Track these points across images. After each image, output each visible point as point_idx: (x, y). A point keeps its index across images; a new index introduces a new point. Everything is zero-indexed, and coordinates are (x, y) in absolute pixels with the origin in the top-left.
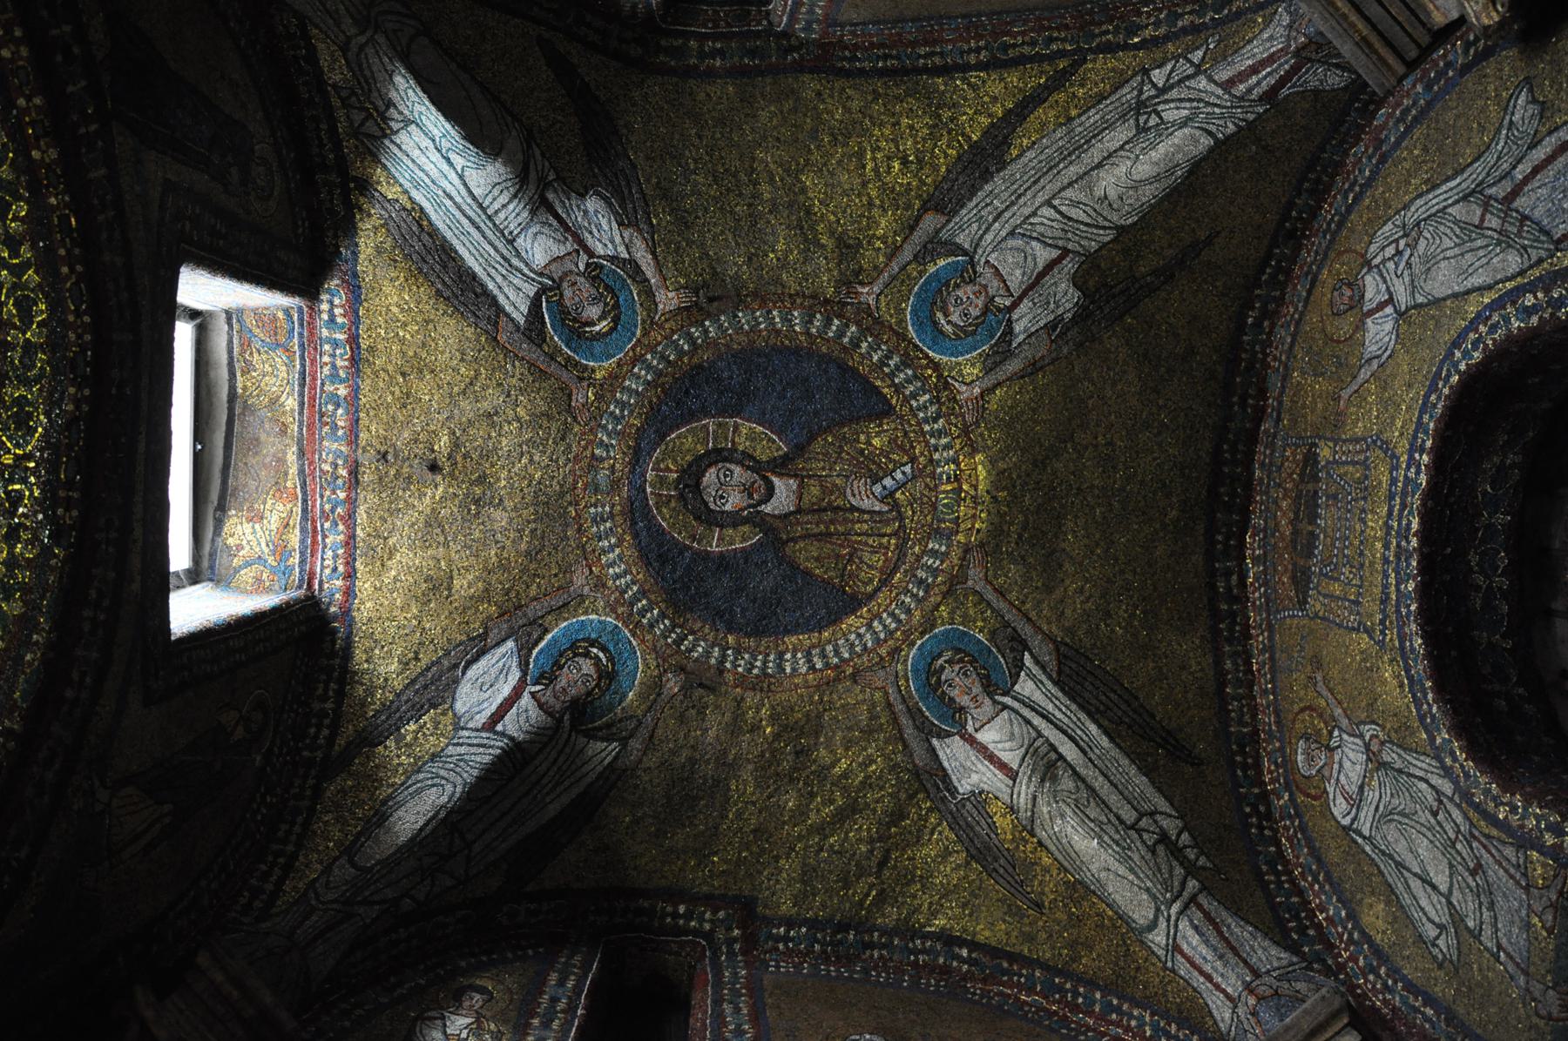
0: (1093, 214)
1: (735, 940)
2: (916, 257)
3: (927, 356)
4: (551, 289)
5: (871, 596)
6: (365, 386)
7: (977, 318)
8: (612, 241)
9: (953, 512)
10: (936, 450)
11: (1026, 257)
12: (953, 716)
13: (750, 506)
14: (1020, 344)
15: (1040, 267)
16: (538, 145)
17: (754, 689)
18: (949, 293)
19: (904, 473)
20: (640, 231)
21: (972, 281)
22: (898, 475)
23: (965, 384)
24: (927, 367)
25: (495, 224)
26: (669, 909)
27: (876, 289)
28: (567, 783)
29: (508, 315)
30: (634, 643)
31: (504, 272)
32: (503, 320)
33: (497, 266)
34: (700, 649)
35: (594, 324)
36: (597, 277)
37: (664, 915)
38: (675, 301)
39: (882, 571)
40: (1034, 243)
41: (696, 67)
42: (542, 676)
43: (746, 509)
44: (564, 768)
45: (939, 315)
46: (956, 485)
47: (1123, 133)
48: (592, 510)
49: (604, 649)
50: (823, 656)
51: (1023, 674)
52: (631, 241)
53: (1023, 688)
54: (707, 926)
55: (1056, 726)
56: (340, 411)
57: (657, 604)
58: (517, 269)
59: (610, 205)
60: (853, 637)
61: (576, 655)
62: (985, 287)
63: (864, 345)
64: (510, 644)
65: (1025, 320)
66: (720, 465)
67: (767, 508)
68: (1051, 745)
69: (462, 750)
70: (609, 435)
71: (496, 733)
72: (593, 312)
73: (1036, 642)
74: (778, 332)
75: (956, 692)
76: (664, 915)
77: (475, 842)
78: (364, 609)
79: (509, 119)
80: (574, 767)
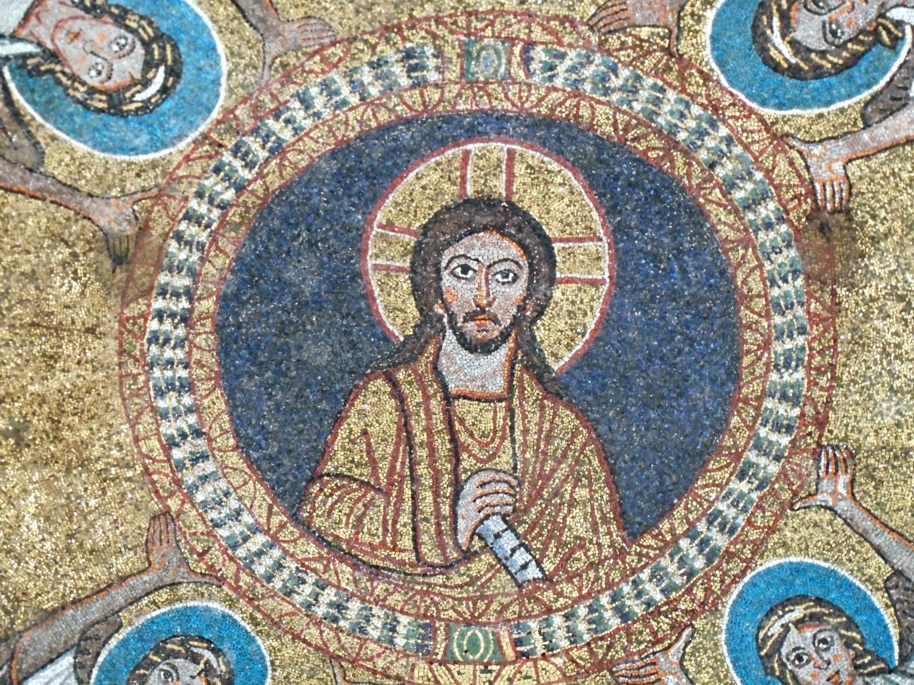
2: (898, 573)
3: (725, 592)
5: (306, 527)
7: (795, 677)
10: (567, 617)
17: (121, 352)
18: (836, 628)
19: (525, 567)
22: (521, 557)
23: (682, 660)
24: (708, 590)
27: (843, 506)
30: (182, 145)
34: (182, 256)
35: (783, 36)
36: (878, 40)
38: (826, 175)
39: (353, 541)
43: (447, 310)
45: (798, 612)
46: (510, 653)
48: (430, 50)
49: (165, 90)
50: (196, 458)
57: (261, 175)
60: (234, 503)
61: (146, 45)
63: (744, 486)
66: (524, 262)
70: (572, 69)
74: (766, 345)
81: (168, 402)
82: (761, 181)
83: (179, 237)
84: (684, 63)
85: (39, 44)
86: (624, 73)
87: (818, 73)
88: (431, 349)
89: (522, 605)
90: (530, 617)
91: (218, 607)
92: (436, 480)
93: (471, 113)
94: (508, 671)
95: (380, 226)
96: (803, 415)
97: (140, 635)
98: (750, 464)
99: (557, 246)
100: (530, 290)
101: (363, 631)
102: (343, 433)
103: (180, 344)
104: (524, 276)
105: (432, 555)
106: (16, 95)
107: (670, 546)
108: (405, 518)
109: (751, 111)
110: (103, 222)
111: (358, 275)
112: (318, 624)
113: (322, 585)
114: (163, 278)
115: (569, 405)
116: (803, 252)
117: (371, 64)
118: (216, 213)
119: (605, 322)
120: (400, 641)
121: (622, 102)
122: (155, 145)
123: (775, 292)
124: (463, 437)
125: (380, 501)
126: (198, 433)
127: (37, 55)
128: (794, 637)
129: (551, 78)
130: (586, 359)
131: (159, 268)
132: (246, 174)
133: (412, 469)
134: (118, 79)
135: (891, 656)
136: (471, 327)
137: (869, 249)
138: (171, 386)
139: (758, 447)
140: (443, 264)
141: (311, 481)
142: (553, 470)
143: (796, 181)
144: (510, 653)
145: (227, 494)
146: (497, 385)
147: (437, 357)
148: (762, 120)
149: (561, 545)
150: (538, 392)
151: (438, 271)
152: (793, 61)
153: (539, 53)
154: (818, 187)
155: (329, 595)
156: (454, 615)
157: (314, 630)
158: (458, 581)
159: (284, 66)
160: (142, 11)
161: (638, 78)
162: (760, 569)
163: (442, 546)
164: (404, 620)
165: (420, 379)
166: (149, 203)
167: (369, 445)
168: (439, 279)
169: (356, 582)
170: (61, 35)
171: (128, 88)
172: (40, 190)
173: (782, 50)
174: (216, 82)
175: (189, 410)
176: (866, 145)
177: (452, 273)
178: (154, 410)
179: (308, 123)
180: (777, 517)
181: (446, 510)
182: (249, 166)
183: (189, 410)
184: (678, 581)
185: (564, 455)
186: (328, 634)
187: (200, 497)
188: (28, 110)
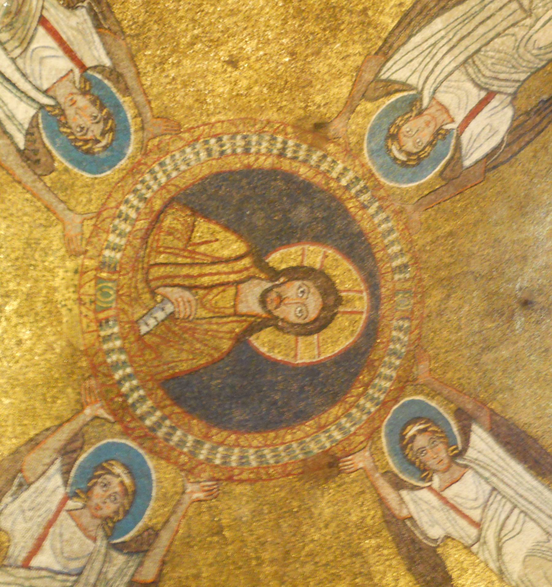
2: (157, 534)
3: (135, 439)
4: (456, 456)
5: (167, 205)
7: (95, 484)
9: (101, 289)
12: (91, 87)
17: (269, 122)
18: (123, 505)
19: (147, 325)
20: (394, 516)
22: (152, 322)
24: (134, 429)
28: (425, 46)
31: (492, 464)
33: (500, 469)
44: (428, 59)
45: (127, 481)
46: (102, 316)
48: (408, 276)
49: (395, 159)
50: (209, 152)
51: (26, 126)
53: (26, 112)
61: (416, 153)
64: (467, 163)
66: (307, 320)
67: (267, 285)
68: (5, 49)
70: (399, 339)
71: (486, 89)
72: (422, 441)
80: (420, 59)
81: (239, 142)
82: (350, 431)
83: (325, 157)
85: (426, 109)
87: (404, 448)
88: (262, 276)
89: (128, 323)
90: (122, 328)
91: (130, 150)
93: (380, 294)
94: (91, 315)
95: (325, 252)
96: (233, 469)
100: (293, 325)
101: (113, 231)
102: (218, 228)
103: (270, 151)
104: (300, 321)
105: (156, 272)
106: (398, 95)
108: (172, 259)
109: (382, 421)
110: (336, 123)
111: (300, 241)
112: (117, 207)
114: (304, 147)
116: (318, 455)
117: (401, 250)
118: (334, 175)
119: (275, 363)
120: (107, 253)
121: (385, 362)
122: (372, 152)
123: (295, 445)
124: (215, 291)
125: (181, 245)
126: (222, 153)
127: (421, 107)
128: (115, 481)
130: (256, 354)
131: (311, 145)
132: (353, 191)
133: (197, 264)
134: (403, 139)
135: (113, 539)
136: (273, 295)
138: (248, 143)
140: (305, 282)
141: (192, 209)
142: (197, 340)
143: (352, 447)
144: (102, 316)
145: (188, 165)
146: (242, 308)
147: (259, 278)
148: (379, 427)
151: (303, 279)
152: (407, 437)
153: (406, 324)
154: (350, 458)
155: (133, 214)
156: (121, 284)
157: (113, 204)
159: (401, 212)
160: (432, 153)
162: (146, 457)
164: (118, 255)
165: (247, 269)
167: (210, 242)
168: (297, 279)
169: (140, 230)
171: (399, 143)
172: (353, 97)
174: (397, 181)
176: (373, 476)
177: (300, 287)
178: (237, 133)
179: (376, 221)
180: (176, 463)
181: (177, 281)
185: (206, 345)
186: (112, 212)
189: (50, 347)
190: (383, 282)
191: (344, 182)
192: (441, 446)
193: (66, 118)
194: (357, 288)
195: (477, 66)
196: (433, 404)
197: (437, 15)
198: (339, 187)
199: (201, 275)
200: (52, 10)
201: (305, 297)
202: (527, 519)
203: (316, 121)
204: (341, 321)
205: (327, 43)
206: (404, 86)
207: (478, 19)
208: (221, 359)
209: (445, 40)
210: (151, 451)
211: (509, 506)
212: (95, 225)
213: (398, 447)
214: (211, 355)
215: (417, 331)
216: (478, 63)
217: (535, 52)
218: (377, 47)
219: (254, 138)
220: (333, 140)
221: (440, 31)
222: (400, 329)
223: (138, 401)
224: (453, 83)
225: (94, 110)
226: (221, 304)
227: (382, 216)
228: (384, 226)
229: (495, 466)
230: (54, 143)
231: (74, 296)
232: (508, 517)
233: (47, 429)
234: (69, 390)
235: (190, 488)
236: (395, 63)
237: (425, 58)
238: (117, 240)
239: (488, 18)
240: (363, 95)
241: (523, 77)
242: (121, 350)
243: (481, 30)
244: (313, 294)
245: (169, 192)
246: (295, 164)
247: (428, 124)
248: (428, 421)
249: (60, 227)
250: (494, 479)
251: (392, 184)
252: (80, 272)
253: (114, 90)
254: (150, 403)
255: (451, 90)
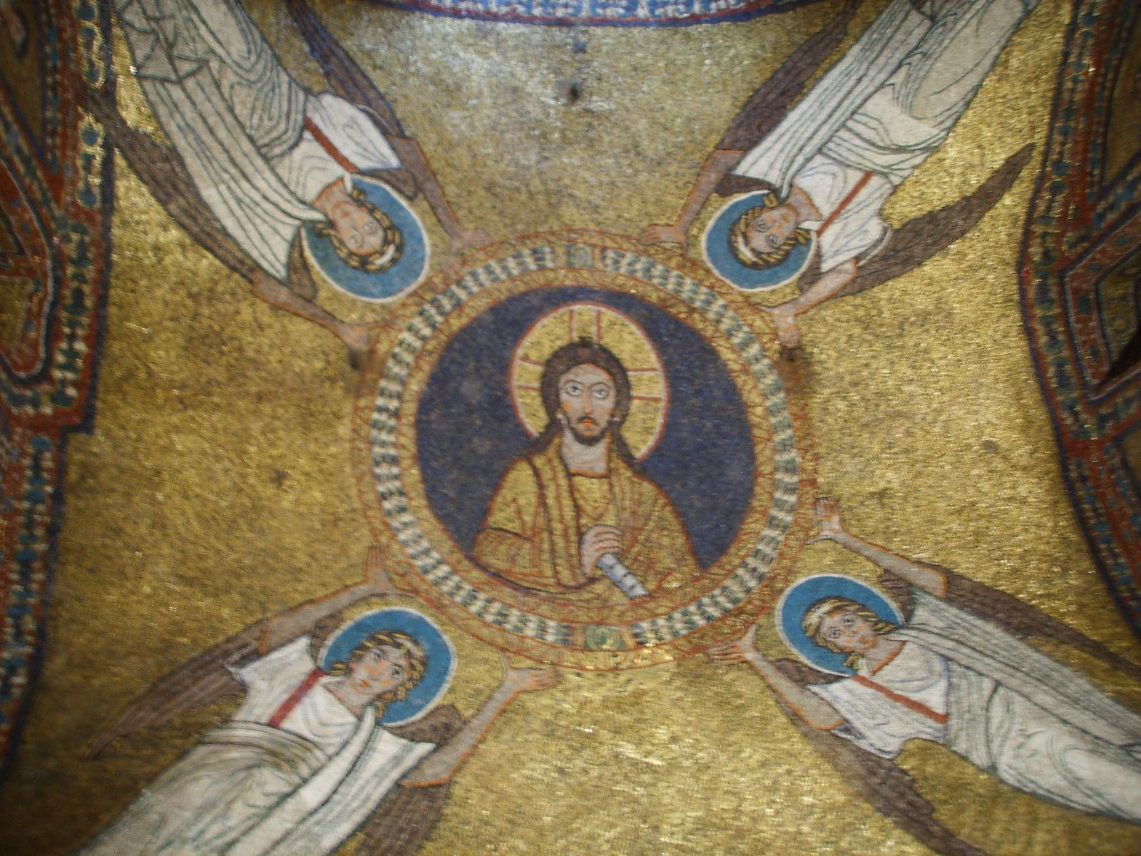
0: (1003, 731)
1: (36, 403)
2: (886, 571)
4: (777, 197)
6: (652, 32)
8: (837, 253)
11: (922, 679)
12: (341, 662)
13: (569, 419)
14: (815, 694)
15: (915, 697)
16: (925, 160)
17: (354, 431)
18: (855, 612)
19: (632, 587)
20: (853, 281)
21: (877, 632)
22: (630, 581)
25: (837, 131)
26: (80, 332)
28: (239, 213)
29: (743, 157)
31: (786, 151)
32: (737, 154)
33: (793, 142)
35: (747, 243)
37: (73, 324)
40: (943, 684)
41: (1033, 317)
42: (362, 192)
44: (258, 210)
45: (826, 607)
46: (631, 642)
47: (1117, 738)
48: (547, 250)
49: (394, 261)
50: (402, 510)
51: (404, 741)
52: (840, 272)
54: (58, 374)
55: (341, 782)
56: (621, 11)
58: (792, 162)
59: (875, 245)
60: (425, 544)
61: (385, 230)
62: (874, 645)
64: (394, 162)
65: (844, 694)
66: (610, 383)
67: (568, 437)
69: (285, 88)
70: (630, 264)
71: (302, 130)
72: (759, 241)
73: (450, 756)
75: (372, 664)
76: (73, 324)
77: (184, 89)
78: (425, 24)
79: (948, 123)
80: (258, 221)
81: (382, 470)
84: (695, 264)
85: (326, 215)
86: (660, 267)
87: (768, 265)
88: (557, 441)
90: (642, 619)
91: (413, 611)
92: (566, 530)
94: (631, 655)
97: (360, 627)
98: (773, 518)
99: (630, 373)
100: (618, 404)
102: (499, 499)
103: (391, 430)
104: (613, 393)
105: (566, 576)
106: (308, 253)
107: (731, 574)
108: (546, 556)
110: (348, 340)
111: (507, 392)
113: (489, 601)
115: (651, 480)
116: (780, 374)
117: (514, 257)
120: (550, 638)
124: (581, 502)
125: (527, 545)
126: (401, 493)
128: (829, 622)
129: (617, 269)
130: (657, 451)
131: (382, 375)
132: (439, 319)
134: (366, 249)
136: (581, 427)
137: (818, 368)
138: (384, 458)
139: (776, 505)
141: (479, 532)
146: (601, 468)
148: (741, 294)
149: (658, 573)
150: (629, 474)
153: (610, 254)
155: (496, 606)
158: (586, 596)
160: (385, 210)
161: (667, 271)
163: (574, 575)
164: (552, 623)
165: (550, 461)
166: (378, 330)
168: (558, 395)
170: (338, 211)
173: (746, 254)
174: (423, 259)
175: (397, 477)
179: (475, 289)
181: (573, 551)
182: (442, 313)
183: (397, 477)
184: (741, 595)
187: (402, 536)
188: (312, 261)
189: (676, 703)
190: (556, 283)
191: (427, 331)
192: (767, 216)
193: (385, 693)
194: (566, 318)
195: (273, 140)
196: (710, 224)
197: (197, 195)
198: (434, 338)
199: (562, 520)
200: (257, 711)
201: (579, 386)
202: (861, 111)
203: (348, 368)
204: (609, 340)
205: (240, 350)
206: (295, 244)
207: (206, 137)
208: (667, 494)
209: (233, 185)
210: (787, 581)
211: (843, 133)
212: (518, 653)
213: (767, 272)
214: (664, 507)
215: (618, 239)
216: (266, 140)
217: (253, 58)
218: (242, 281)
219: (378, 450)
220: (373, 342)
221: (220, 193)
222: (616, 262)
223: (727, 596)
224: (294, 177)
225: (369, 658)
226: (597, 495)
227: (469, 281)
228: (483, 277)
229: (789, 146)
230: (420, 708)
231: (610, 675)
232: (858, 135)
233: (778, 702)
234: (728, 678)
235: (827, 533)
236: (263, 256)
237: (256, 214)
238: (532, 625)
239: (205, 121)
240: (309, 301)
241: (285, 78)
242: (670, 618)
243: (222, 133)
244: (577, 375)
245: (459, 562)
246: (407, 397)
247: (346, 214)
248: (732, 232)
249: (523, 697)
250: (807, 150)
251: (427, 267)
252: (580, 670)
253: (338, 633)
254: (728, 582)
255: (302, 179)
